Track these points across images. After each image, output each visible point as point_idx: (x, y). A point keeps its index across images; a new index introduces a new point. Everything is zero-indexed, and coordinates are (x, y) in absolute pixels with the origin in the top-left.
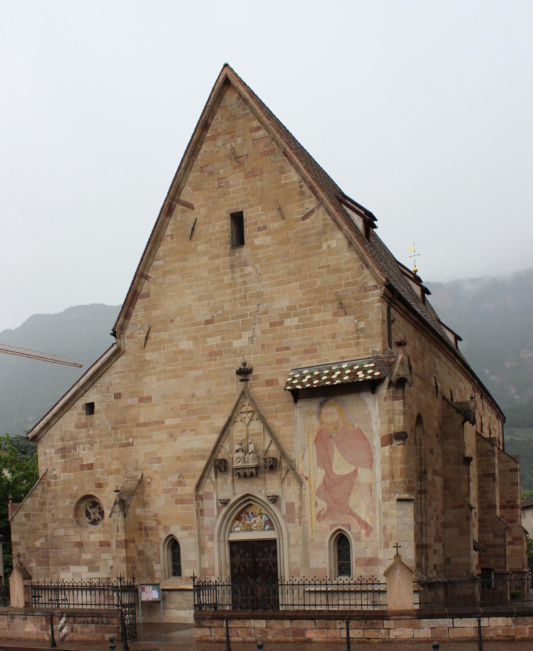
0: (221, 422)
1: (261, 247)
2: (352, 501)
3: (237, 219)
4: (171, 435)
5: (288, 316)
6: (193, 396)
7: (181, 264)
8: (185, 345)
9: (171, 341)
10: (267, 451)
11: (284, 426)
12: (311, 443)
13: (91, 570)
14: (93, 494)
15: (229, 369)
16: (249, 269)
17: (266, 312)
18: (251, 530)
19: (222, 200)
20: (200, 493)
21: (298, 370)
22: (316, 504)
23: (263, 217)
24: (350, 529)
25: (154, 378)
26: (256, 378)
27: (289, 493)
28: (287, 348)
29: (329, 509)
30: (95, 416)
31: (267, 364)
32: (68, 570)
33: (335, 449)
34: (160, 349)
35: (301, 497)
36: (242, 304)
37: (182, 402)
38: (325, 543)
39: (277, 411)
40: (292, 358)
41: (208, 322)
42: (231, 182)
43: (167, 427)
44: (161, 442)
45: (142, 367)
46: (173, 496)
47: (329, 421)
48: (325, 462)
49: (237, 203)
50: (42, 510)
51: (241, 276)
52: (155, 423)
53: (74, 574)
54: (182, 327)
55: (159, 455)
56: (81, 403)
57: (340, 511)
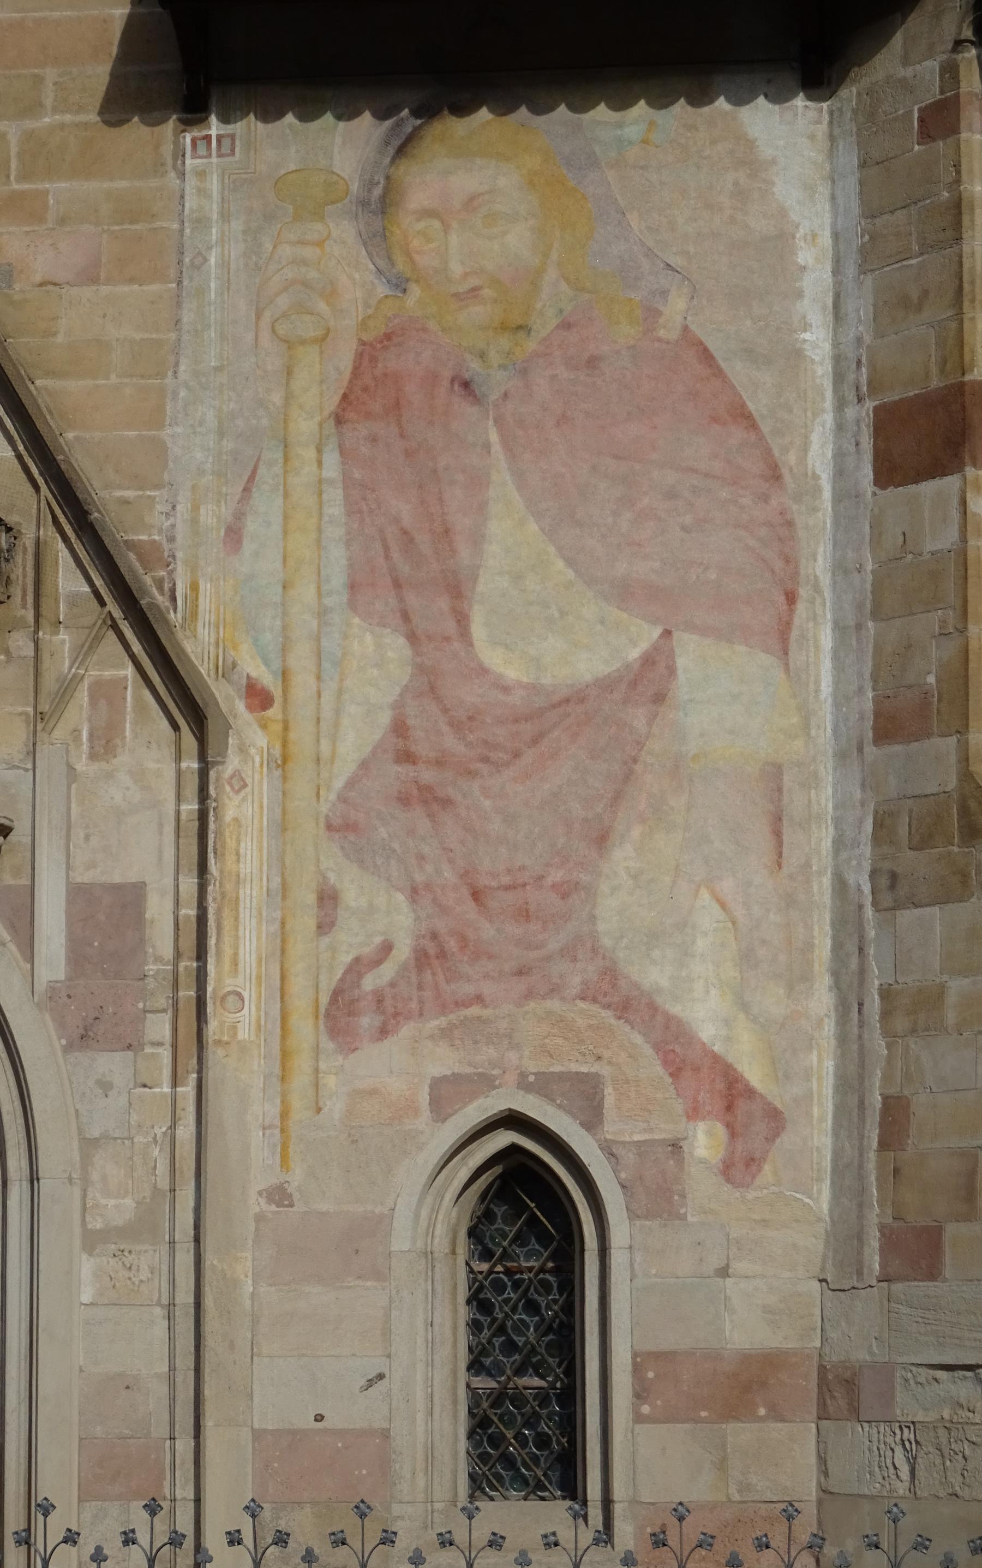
2: (619, 900)
11: (90, 276)
12: (305, 426)
22: (328, 899)
24: (592, 1120)
35: (201, 840)
38: (378, 1226)
39: (40, 158)
47: (456, 269)
48: (416, 577)
57: (520, 972)
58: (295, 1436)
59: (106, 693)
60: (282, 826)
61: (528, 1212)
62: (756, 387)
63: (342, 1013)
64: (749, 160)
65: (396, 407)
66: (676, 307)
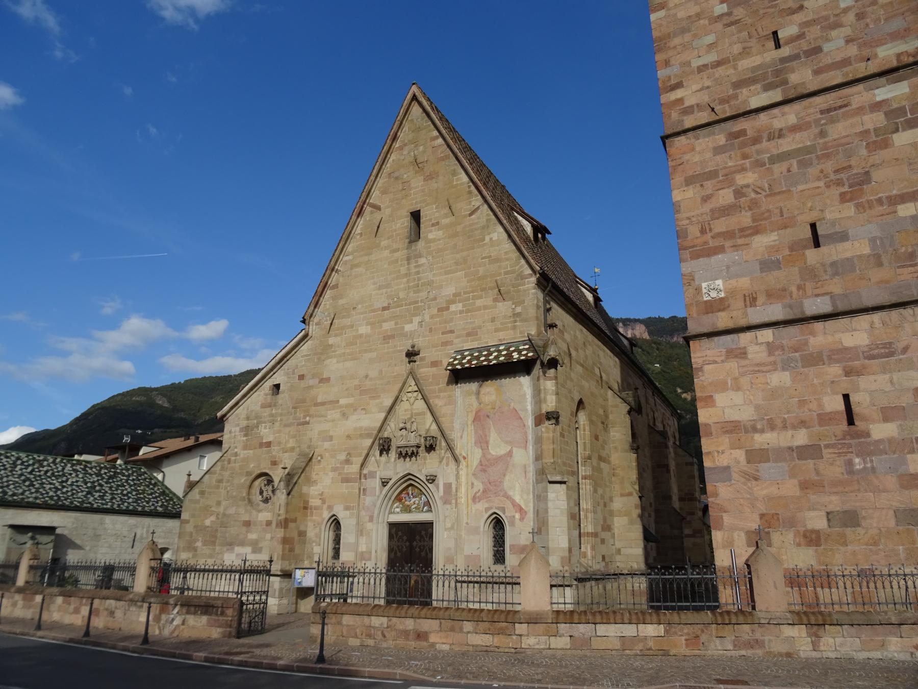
0: (388, 402)
1: (434, 240)
2: (507, 483)
3: (416, 216)
5: (453, 302)
7: (366, 258)
8: (364, 330)
9: (352, 326)
10: (428, 430)
11: (445, 405)
12: (470, 423)
13: (254, 551)
14: (267, 471)
15: (400, 351)
16: (423, 261)
17: (435, 299)
19: (404, 201)
20: (365, 471)
21: (461, 352)
22: (473, 484)
23: (437, 215)
25: (335, 360)
26: (423, 359)
28: (452, 332)
30: (280, 396)
31: (434, 346)
33: (492, 428)
34: (341, 334)
35: (458, 477)
36: (415, 292)
37: (357, 382)
38: (479, 527)
39: (440, 391)
40: (456, 341)
41: (384, 309)
42: (412, 185)
43: (341, 407)
44: (333, 420)
45: (325, 351)
46: (340, 474)
48: (482, 441)
49: (416, 203)
50: (218, 487)
51: (415, 267)
52: (331, 402)
54: (362, 313)
55: (331, 433)
58: (469, 556)
59: (448, 458)
60: (467, 475)
61: (498, 524)
62: (522, 414)
63: (475, 499)
64: (521, 385)
65: (480, 420)
66: (512, 405)
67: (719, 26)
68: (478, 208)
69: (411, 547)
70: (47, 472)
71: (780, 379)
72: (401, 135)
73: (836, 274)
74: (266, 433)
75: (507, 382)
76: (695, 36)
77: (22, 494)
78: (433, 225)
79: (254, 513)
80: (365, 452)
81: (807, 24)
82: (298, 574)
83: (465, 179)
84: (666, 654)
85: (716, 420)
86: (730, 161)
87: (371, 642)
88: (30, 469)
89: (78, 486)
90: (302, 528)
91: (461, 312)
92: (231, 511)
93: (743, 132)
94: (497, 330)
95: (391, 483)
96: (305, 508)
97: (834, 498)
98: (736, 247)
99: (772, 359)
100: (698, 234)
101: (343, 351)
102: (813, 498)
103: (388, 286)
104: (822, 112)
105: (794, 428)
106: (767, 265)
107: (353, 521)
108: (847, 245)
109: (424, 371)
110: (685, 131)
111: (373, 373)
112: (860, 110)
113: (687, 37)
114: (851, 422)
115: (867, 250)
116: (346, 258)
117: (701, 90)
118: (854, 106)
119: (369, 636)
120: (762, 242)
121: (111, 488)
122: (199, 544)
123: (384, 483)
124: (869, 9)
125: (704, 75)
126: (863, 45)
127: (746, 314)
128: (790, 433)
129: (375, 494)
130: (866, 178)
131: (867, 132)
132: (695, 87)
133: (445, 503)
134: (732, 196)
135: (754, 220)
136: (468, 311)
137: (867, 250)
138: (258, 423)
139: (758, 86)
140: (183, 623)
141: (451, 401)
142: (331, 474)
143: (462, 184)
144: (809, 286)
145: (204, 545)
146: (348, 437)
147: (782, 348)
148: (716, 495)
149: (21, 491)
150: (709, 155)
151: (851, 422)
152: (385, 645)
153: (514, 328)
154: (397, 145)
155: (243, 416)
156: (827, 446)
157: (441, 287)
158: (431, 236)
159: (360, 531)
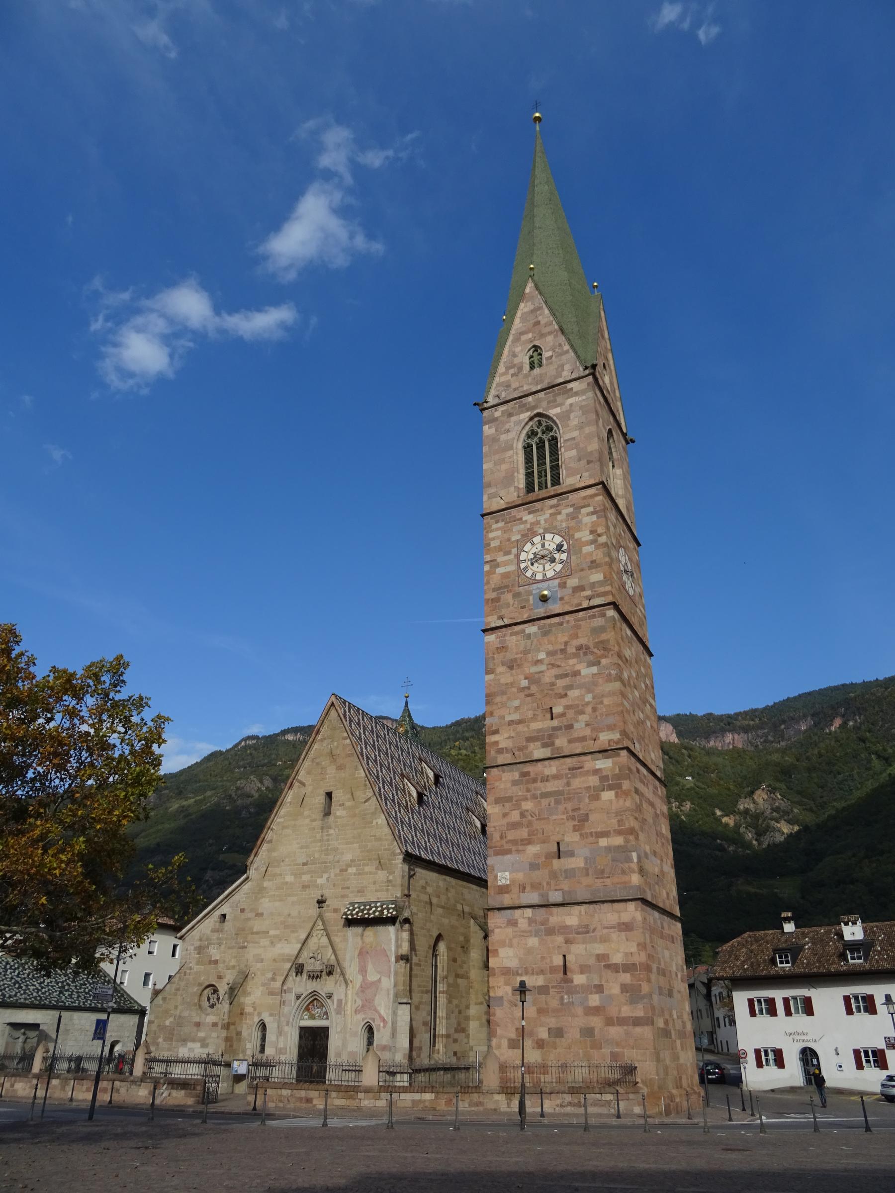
0: (303, 936)
2: (376, 1002)
3: (329, 795)
4: (272, 943)
5: (350, 866)
6: (289, 915)
7: (293, 823)
8: (289, 878)
10: (329, 960)
15: (313, 898)
16: (331, 831)
17: (338, 862)
18: (314, 1019)
20: (285, 988)
21: (352, 904)
25: (267, 900)
26: (328, 906)
27: (339, 992)
28: (348, 888)
29: (363, 1006)
30: (226, 924)
32: (185, 1045)
35: (346, 994)
36: (326, 855)
40: (351, 895)
41: (304, 864)
45: (260, 891)
48: (363, 971)
50: (176, 994)
53: (190, 1049)
54: (289, 865)
56: (217, 913)
61: (370, 1030)
67: (522, 695)
68: (370, 798)
69: (314, 1044)
70: (29, 974)
71: (533, 942)
72: (322, 730)
73: (566, 877)
74: (214, 953)
75: (381, 929)
76: (509, 698)
77: (15, 996)
78: (340, 805)
79: (203, 1016)
80: (286, 973)
81: (567, 707)
82: (236, 1064)
83: (363, 774)
84: (435, 1109)
85: (498, 965)
86: (519, 791)
87: (281, 1105)
88: (17, 972)
89: (52, 986)
90: (239, 1029)
91: (355, 874)
92: (186, 1014)
93: (527, 774)
94: (377, 891)
95: (302, 997)
96: (242, 1014)
97: (553, 1020)
98: (518, 851)
99: (530, 928)
100: (499, 839)
101: (273, 893)
102: (543, 1019)
103: (307, 847)
104: (570, 769)
105: (537, 974)
106: (534, 866)
107: (275, 1025)
108: (573, 859)
109: (329, 915)
110: (497, 766)
111: (294, 913)
112: (587, 773)
113: (505, 698)
114: (565, 973)
115: (582, 865)
116: (279, 820)
117: (509, 738)
118: (585, 769)
119: (281, 1101)
120: (533, 849)
121: (76, 986)
122: (160, 1040)
123: (298, 997)
124: (599, 706)
125: (512, 727)
126: (593, 730)
127: (519, 897)
128: (535, 977)
129: (291, 1006)
130: (585, 818)
131: (590, 787)
132: (506, 735)
133: (337, 1014)
134: (518, 816)
135: (529, 835)
136: (359, 874)
137: (582, 865)
138: (209, 944)
139: (538, 744)
140: (169, 1095)
141: (345, 940)
142: (261, 988)
143: (361, 778)
144: (553, 882)
145: (164, 1040)
146: (274, 960)
147: (535, 922)
148: (494, 1015)
149: (14, 993)
150: (509, 785)
151: (565, 973)
152: (289, 1106)
153: (387, 890)
154: (319, 737)
155: (197, 938)
156: (553, 987)
157: (343, 853)
158: (338, 814)
159: (280, 1033)
